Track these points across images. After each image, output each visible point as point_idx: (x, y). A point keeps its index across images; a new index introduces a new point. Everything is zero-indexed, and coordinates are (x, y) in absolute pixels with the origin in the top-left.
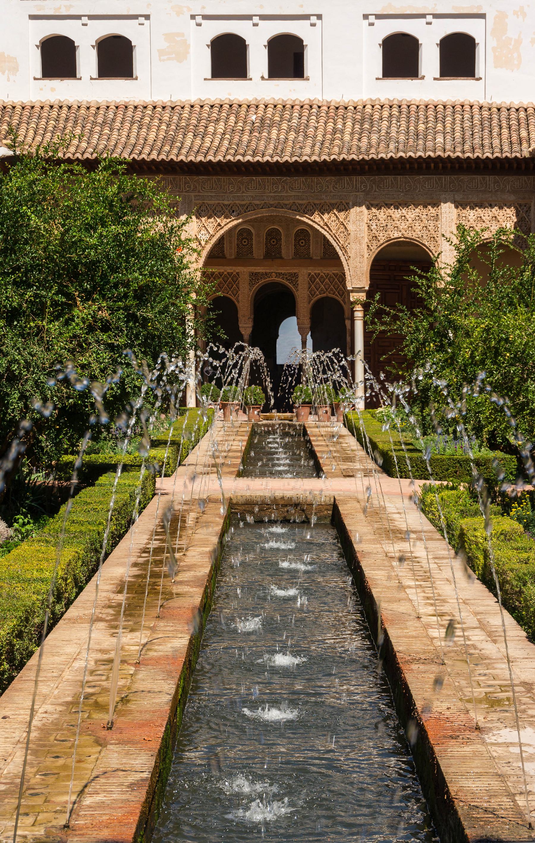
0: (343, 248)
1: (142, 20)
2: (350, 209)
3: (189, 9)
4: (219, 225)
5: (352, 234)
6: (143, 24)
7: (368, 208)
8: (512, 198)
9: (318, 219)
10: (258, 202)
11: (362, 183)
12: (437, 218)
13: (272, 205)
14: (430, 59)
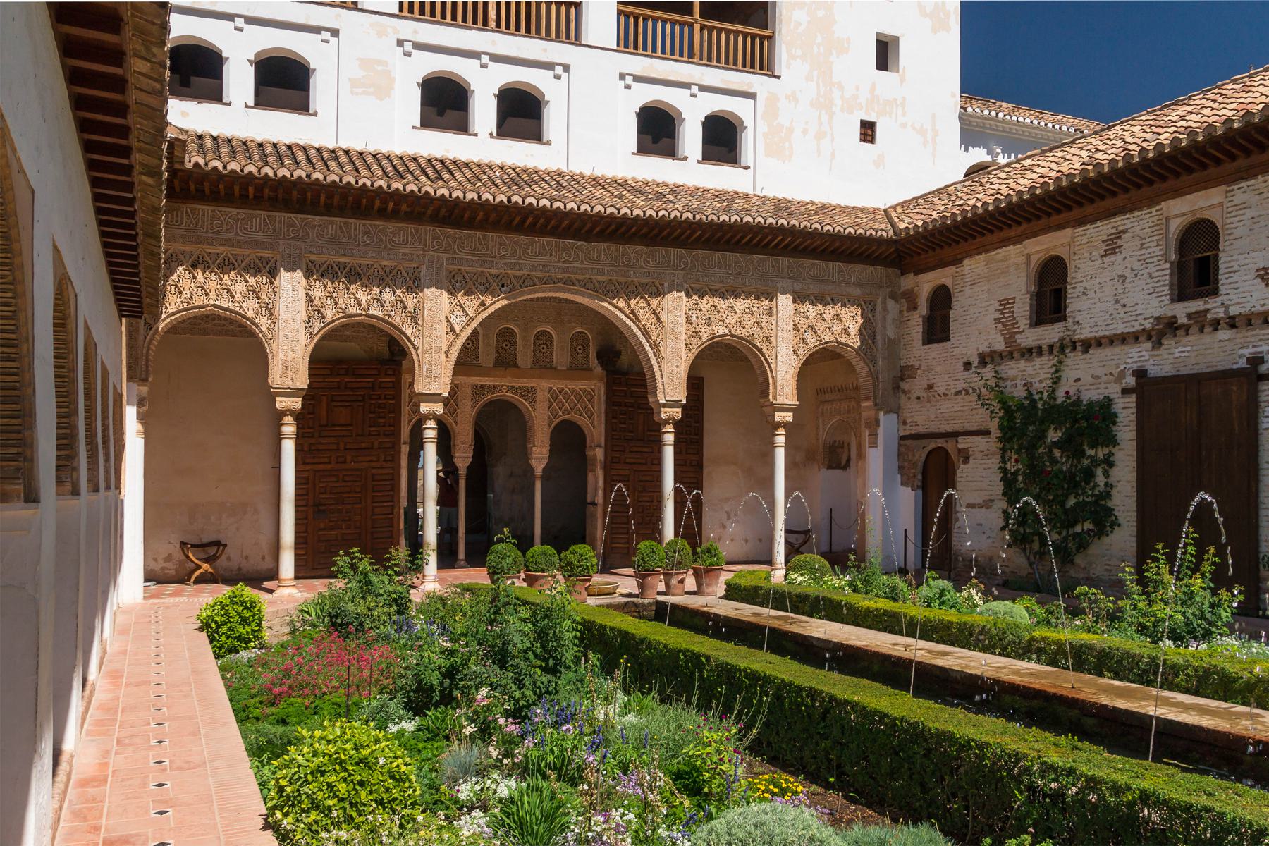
0: (655, 346)
1: (326, 35)
2: (665, 294)
3: (396, 31)
4: (483, 304)
5: (668, 327)
6: (327, 42)
7: (688, 295)
8: (858, 292)
9: (621, 304)
10: (540, 274)
11: (681, 258)
12: (770, 312)
13: (560, 280)
14: (691, 138)
